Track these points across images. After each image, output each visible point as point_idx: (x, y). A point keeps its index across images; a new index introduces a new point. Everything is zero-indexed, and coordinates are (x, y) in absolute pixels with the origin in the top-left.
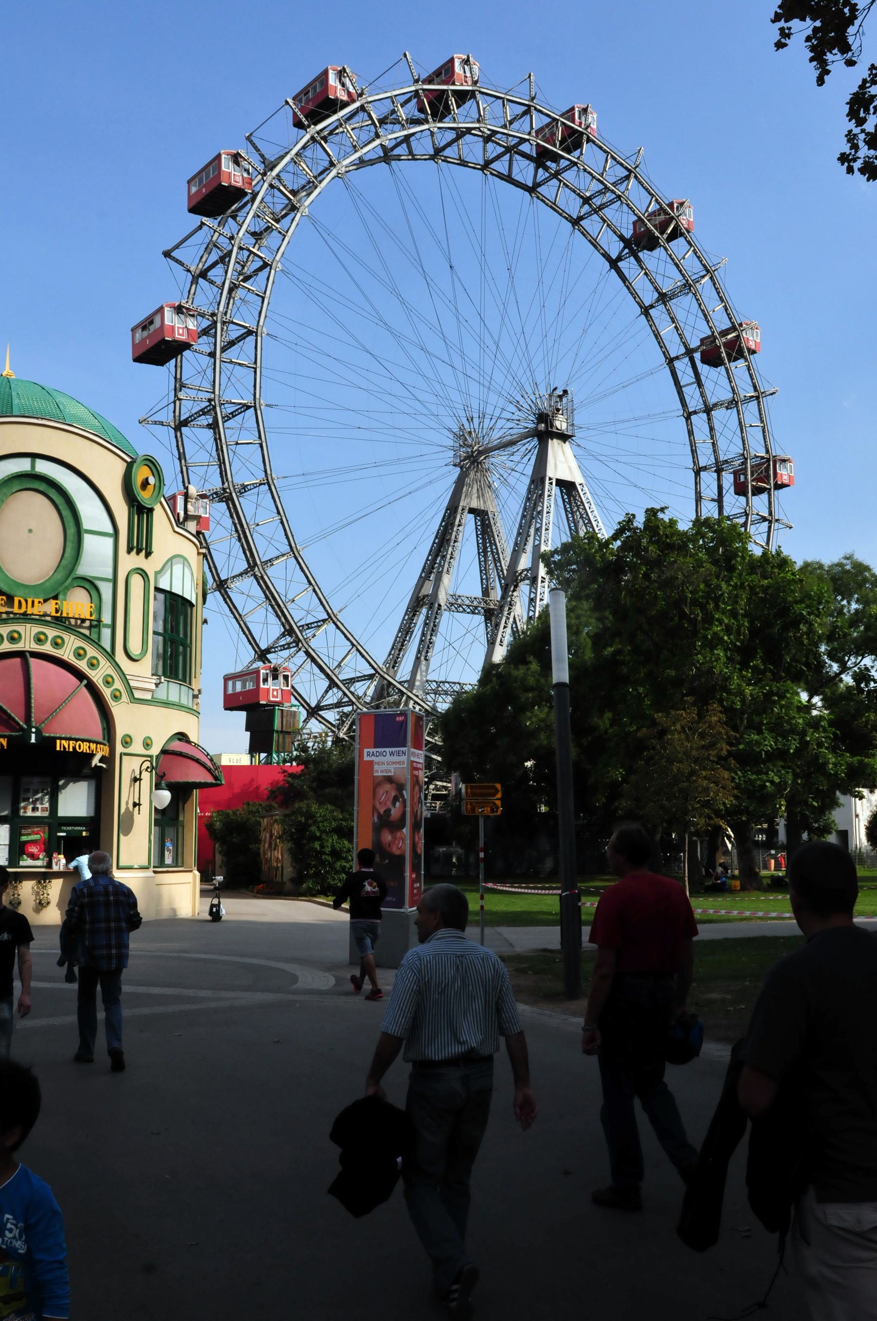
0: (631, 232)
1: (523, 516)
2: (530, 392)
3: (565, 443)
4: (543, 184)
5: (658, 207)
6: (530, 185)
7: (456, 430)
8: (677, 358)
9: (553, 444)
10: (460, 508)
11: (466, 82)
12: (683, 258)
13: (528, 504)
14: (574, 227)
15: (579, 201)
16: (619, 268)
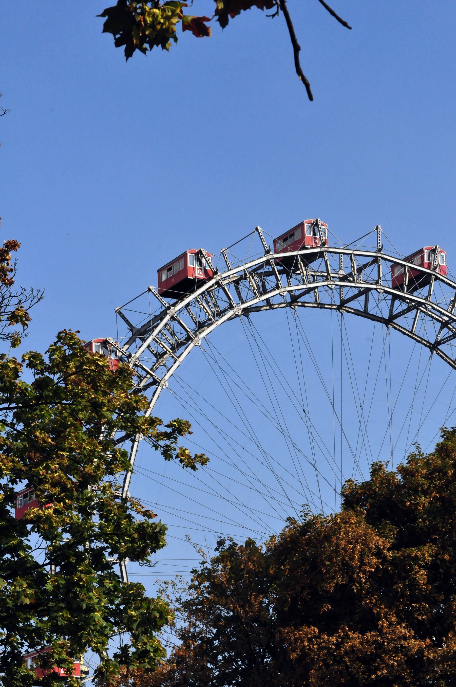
6: (386, 317)
11: (316, 243)
14: (432, 352)
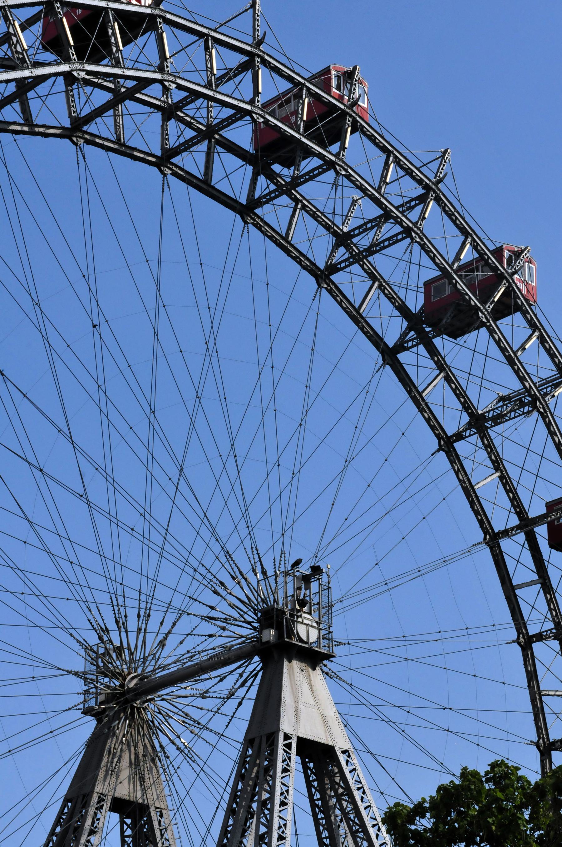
0: (421, 301)
1: (231, 812)
2: (246, 568)
3: (314, 669)
4: (267, 202)
5: (476, 255)
7: (93, 639)
8: (506, 533)
9: (291, 670)
10: (95, 798)
12: (523, 348)
13: (240, 786)
15: (328, 240)
16: (401, 364)
